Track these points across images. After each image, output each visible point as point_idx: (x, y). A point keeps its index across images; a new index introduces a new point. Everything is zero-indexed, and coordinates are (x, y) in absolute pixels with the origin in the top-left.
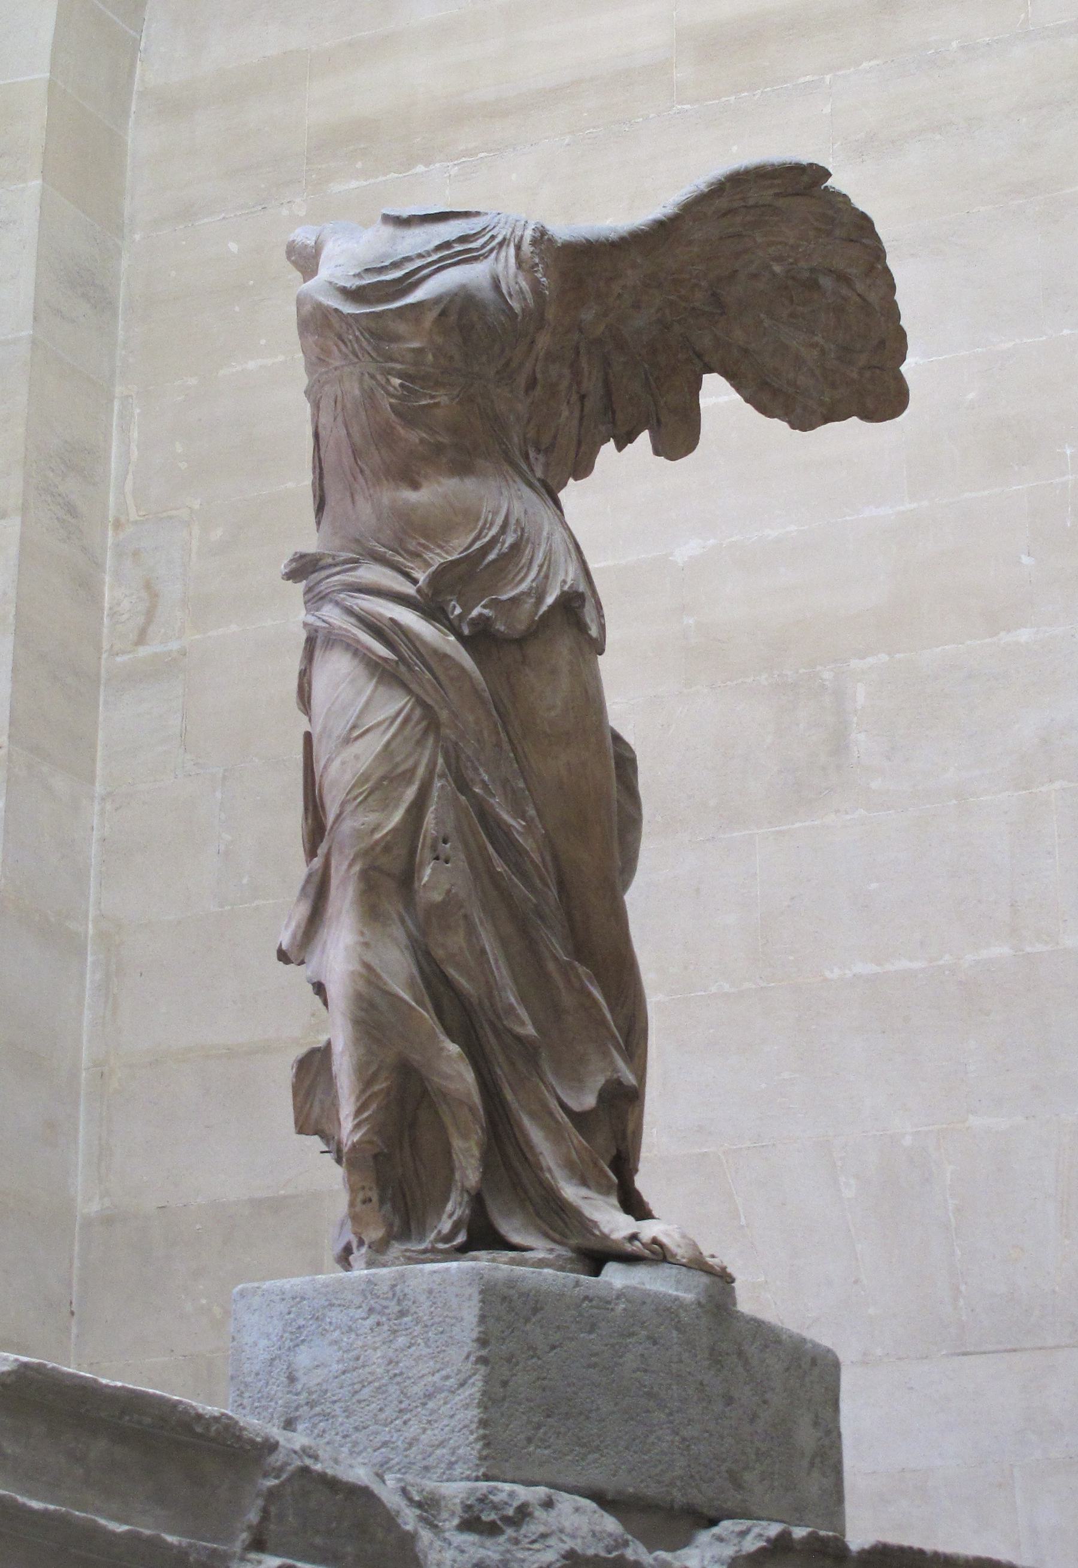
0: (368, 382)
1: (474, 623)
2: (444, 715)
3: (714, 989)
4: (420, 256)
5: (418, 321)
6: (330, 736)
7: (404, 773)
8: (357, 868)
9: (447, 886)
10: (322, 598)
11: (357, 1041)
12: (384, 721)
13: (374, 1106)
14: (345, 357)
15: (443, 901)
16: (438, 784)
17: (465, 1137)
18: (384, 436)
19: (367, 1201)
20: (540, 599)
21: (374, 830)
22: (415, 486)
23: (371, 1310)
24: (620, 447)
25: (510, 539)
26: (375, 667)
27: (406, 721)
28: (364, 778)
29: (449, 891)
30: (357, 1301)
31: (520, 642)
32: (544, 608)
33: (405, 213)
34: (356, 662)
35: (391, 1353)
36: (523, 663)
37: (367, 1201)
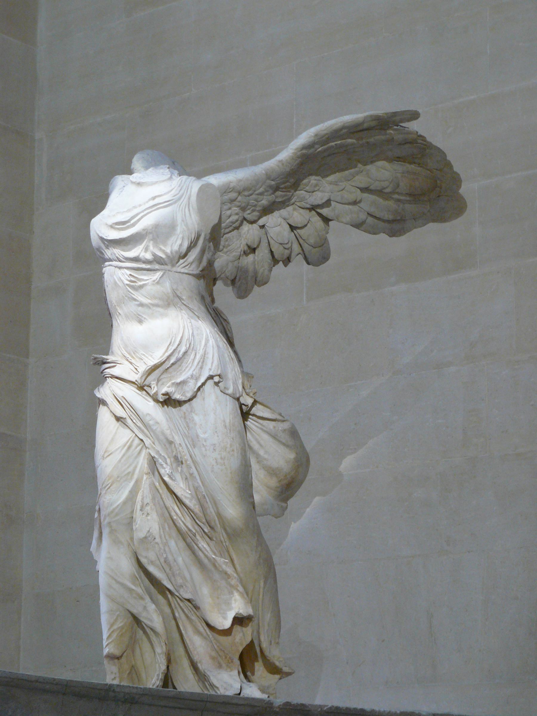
1: (163, 395)
2: (147, 442)
4: (140, 205)
7: (129, 473)
9: (148, 529)
12: (119, 448)
13: (115, 635)
15: (145, 538)
16: (145, 477)
20: (197, 379)
24: (286, 266)
25: (183, 349)
26: (118, 419)
27: (129, 448)
29: (149, 531)
31: (190, 400)
32: (199, 384)
36: (191, 411)
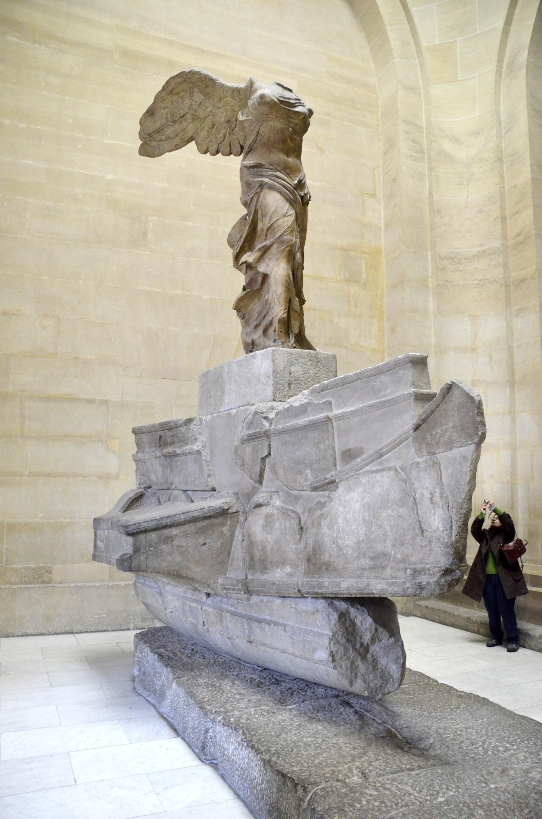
0: (283, 126)
3: (109, 284)
5: (298, 116)
6: (278, 213)
8: (288, 249)
10: (262, 176)
11: (285, 292)
14: (277, 116)
17: (295, 320)
18: (284, 141)
19: (281, 331)
21: (292, 241)
22: (288, 157)
23: (310, 360)
28: (290, 227)
30: (307, 357)
33: (285, 86)
34: (282, 197)
35: (315, 371)
37: (281, 331)
